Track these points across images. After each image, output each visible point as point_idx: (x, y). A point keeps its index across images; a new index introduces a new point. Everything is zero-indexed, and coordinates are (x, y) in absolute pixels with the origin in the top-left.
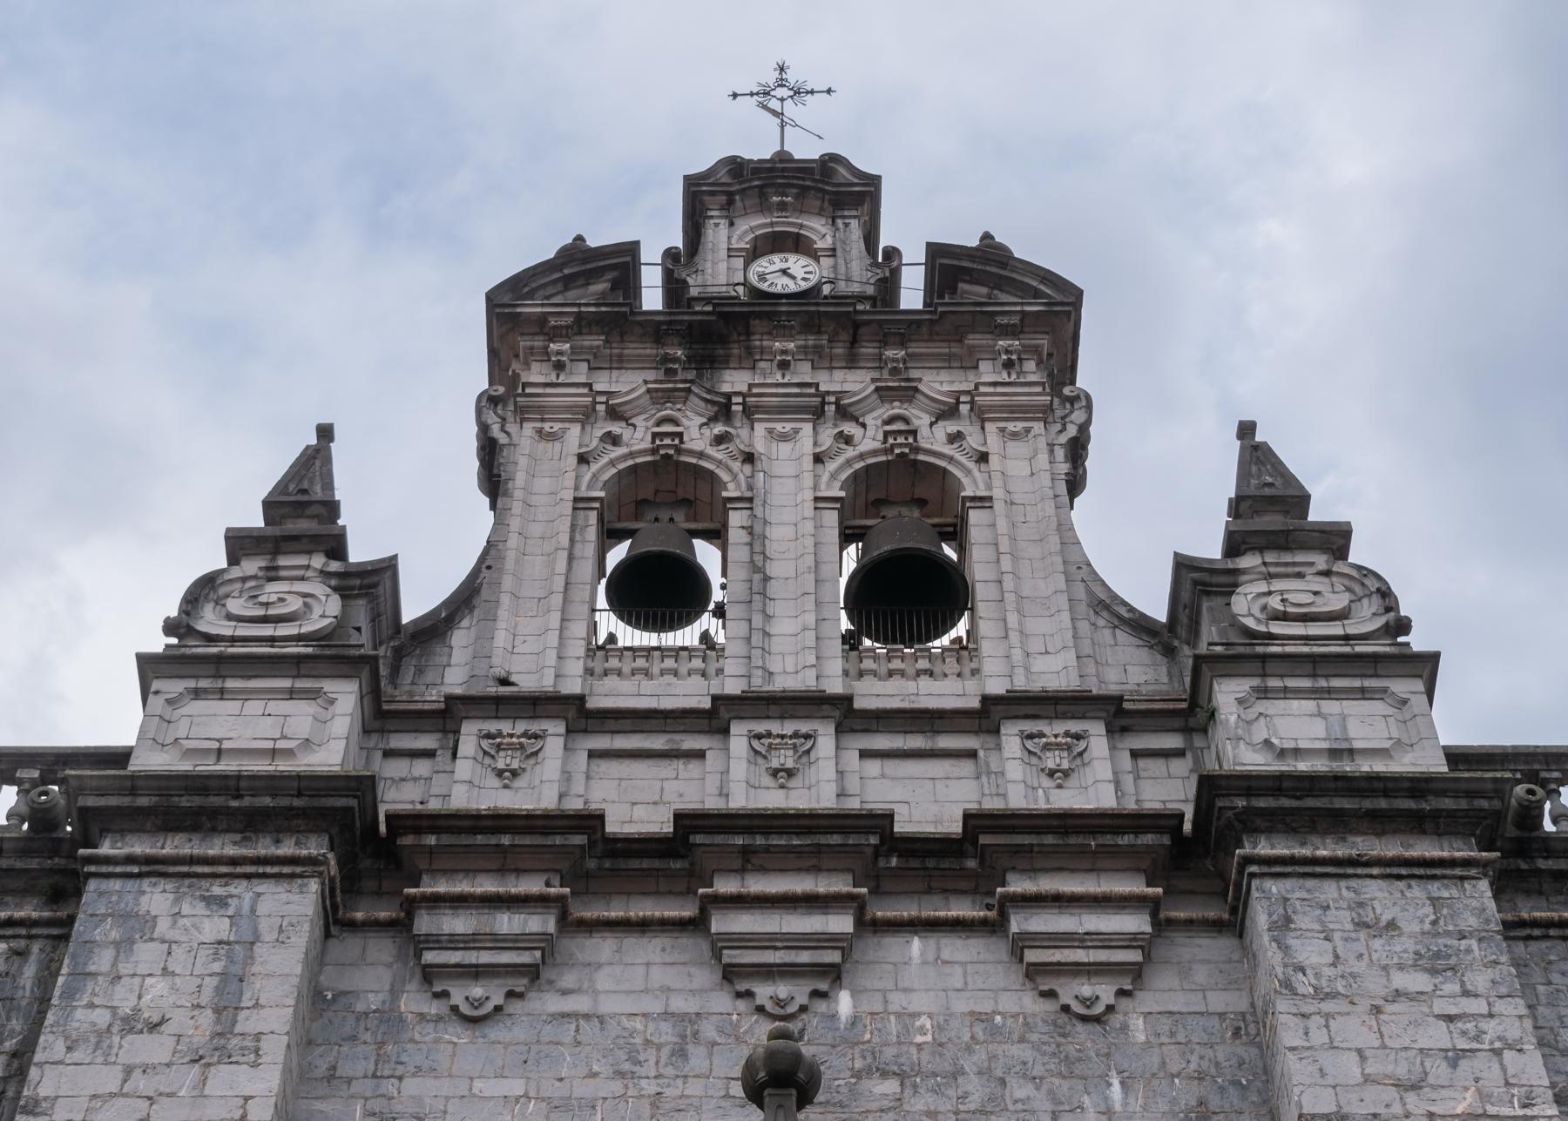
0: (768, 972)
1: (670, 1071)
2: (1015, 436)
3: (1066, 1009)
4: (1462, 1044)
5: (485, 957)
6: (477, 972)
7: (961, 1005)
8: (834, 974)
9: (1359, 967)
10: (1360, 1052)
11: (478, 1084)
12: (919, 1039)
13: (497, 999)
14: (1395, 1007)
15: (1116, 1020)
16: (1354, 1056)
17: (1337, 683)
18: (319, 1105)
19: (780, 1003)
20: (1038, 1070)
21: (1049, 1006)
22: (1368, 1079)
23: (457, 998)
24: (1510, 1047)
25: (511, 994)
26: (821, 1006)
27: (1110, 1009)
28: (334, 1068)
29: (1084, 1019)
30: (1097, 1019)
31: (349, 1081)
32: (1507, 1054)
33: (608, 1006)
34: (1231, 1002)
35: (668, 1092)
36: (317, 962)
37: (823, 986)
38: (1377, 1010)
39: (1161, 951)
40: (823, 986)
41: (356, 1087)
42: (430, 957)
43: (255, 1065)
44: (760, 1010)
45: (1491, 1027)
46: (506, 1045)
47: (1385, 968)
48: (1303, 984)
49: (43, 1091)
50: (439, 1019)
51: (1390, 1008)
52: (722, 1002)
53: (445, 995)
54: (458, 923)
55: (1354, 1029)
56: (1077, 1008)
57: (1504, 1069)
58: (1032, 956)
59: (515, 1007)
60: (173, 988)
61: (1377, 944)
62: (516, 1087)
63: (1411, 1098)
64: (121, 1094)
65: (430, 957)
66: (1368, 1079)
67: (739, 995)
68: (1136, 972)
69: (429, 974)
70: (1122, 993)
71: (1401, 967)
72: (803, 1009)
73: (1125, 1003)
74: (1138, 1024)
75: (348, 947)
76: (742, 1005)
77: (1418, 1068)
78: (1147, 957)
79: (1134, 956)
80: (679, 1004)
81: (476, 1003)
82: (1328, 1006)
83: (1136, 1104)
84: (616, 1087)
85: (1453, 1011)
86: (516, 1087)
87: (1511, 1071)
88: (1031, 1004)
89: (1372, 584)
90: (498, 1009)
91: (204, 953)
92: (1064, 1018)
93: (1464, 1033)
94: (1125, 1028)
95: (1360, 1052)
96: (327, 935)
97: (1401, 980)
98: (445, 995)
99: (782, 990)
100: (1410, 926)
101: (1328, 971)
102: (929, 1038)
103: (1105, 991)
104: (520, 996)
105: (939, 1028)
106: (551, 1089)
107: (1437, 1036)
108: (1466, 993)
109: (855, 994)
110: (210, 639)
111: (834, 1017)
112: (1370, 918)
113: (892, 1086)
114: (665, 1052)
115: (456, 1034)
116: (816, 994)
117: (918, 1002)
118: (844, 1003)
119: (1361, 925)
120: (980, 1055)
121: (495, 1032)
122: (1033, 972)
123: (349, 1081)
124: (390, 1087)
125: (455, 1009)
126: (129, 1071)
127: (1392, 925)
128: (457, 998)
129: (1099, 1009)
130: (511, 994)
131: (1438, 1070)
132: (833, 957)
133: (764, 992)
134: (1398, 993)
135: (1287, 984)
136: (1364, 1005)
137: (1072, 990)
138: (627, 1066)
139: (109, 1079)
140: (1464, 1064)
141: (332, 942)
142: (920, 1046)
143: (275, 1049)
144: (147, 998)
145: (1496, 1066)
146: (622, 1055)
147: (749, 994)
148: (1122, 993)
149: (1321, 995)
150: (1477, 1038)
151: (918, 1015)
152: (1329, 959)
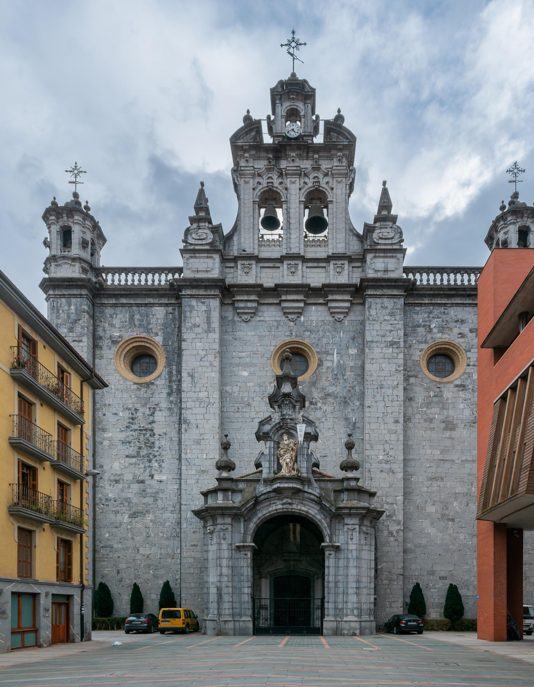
2: (339, 182)
17: (388, 255)
20: (331, 330)
30: (340, 321)
34: (360, 318)
49: (185, 337)
54: (242, 305)
61: (384, 311)
83: (344, 336)
89: (399, 231)
91: (203, 313)
100: (389, 307)
101: (375, 316)
110: (191, 244)
112: (383, 306)
124: (235, 333)
126: (196, 334)
128: (243, 318)
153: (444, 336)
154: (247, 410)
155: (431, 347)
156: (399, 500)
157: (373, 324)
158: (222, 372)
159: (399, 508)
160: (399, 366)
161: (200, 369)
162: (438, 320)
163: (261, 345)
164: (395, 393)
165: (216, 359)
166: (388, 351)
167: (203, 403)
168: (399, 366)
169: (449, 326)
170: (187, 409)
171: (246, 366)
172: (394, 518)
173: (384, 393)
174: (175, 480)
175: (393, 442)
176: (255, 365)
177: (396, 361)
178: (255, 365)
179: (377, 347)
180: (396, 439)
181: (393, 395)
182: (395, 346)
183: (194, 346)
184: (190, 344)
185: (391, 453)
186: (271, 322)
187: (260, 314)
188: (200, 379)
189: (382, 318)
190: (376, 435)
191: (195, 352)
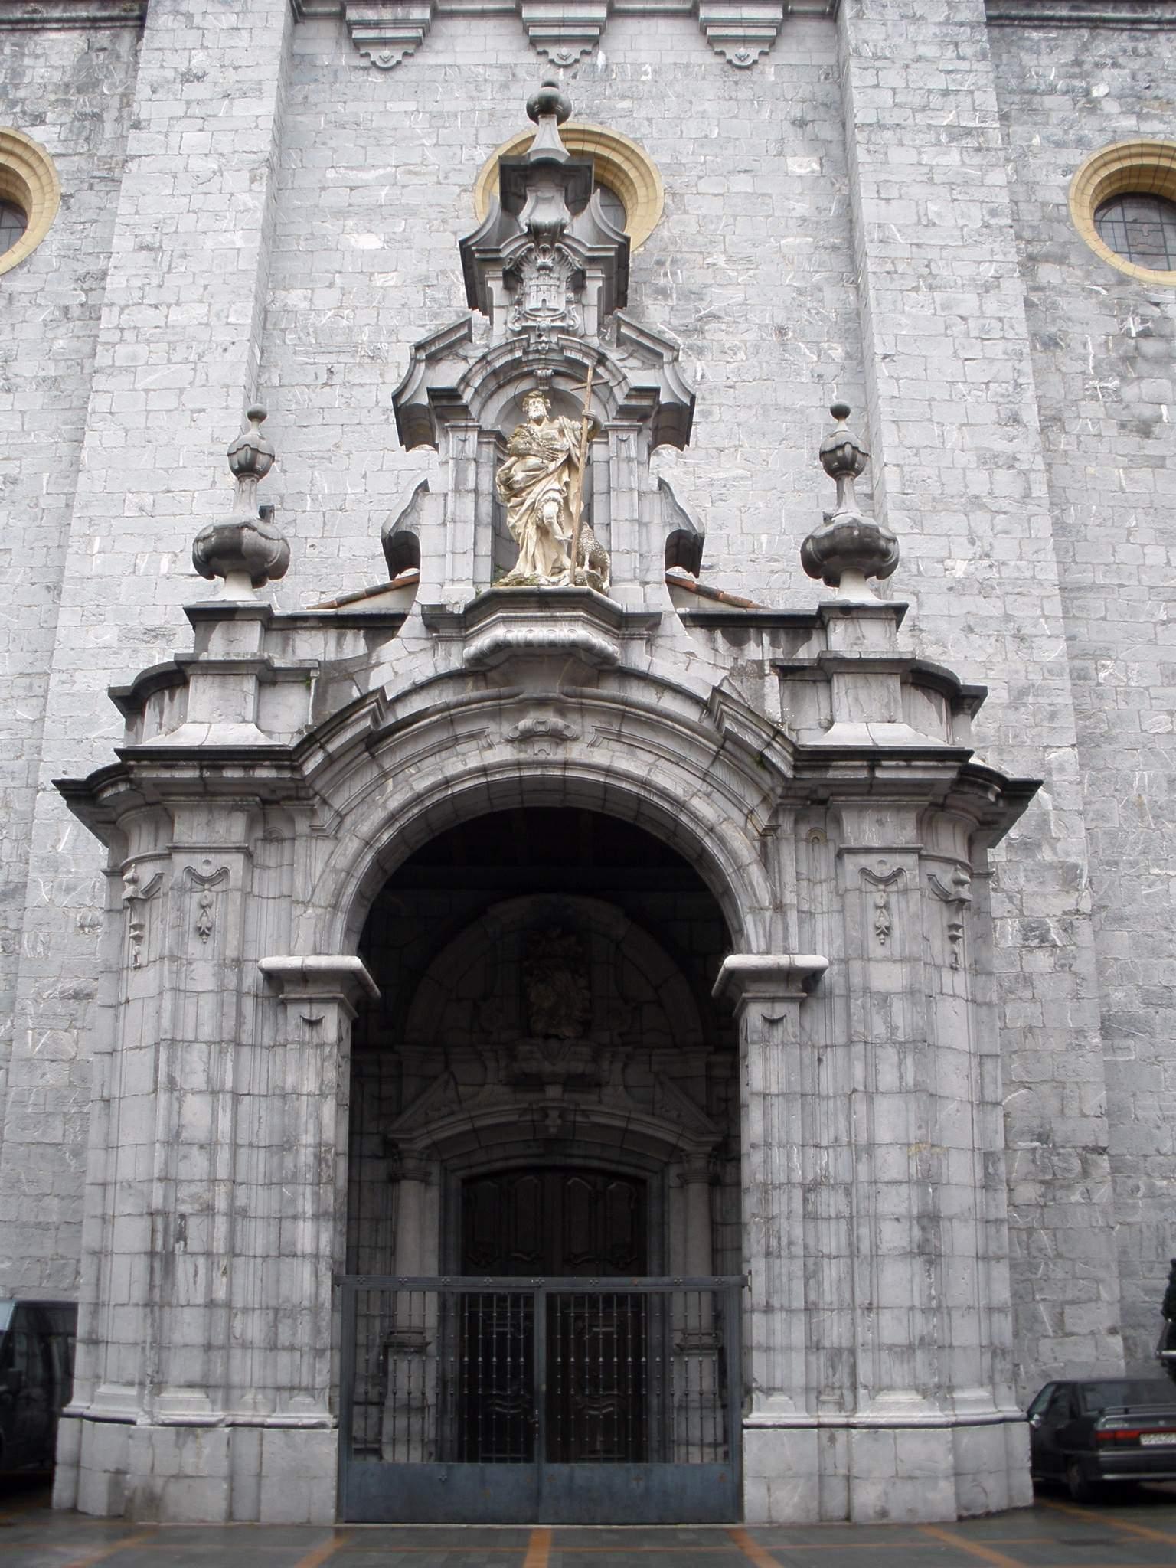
0: (559, 40)
1: (498, 96)
3: (730, 62)
4: (952, 87)
5: (389, 34)
6: (385, 42)
7: (669, 59)
8: (595, 41)
9: (900, 41)
10: (894, 90)
11: (389, 105)
12: (644, 78)
13: (398, 57)
14: (918, 65)
15: (757, 69)
16: (890, 93)
18: (299, 118)
19: (562, 58)
21: (720, 60)
22: (896, 105)
23: (374, 57)
24: (978, 89)
25: (405, 54)
26: (587, 60)
27: (755, 62)
28: (306, 97)
29: (740, 68)
31: (316, 105)
32: (977, 93)
33: (460, 62)
35: (498, 107)
36: (290, 37)
37: (588, 48)
38: (907, 66)
39: (788, 29)
40: (588, 48)
41: (319, 108)
42: (358, 34)
43: (260, 98)
44: (552, 61)
45: (970, 79)
46: (404, 83)
47: (915, 43)
48: (867, 51)
50: (364, 69)
51: (913, 65)
52: (530, 57)
53: (367, 55)
55: (893, 77)
56: (736, 62)
57: (974, 102)
58: (711, 32)
59: (408, 61)
60: (209, 56)
61: (912, 29)
62: (411, 106)
63: (919, 116)
64: (186, 116)
65: (358, 34)
66: (896, 105)
67: (539, 53)
68: (772, 42)
69: (357, 44)
70: (762, 53)
71: (924, 42)
72: (577, 61)
73: (763, 59)
74: (770, 71)
75: (311, 28)
76: (542, 59)
77: (925, 99)
78: (779, 32)
79: (772, 32)
80: (504, 59)
81: (385, 60)
82: (878, 64)
84: (469, 105)
85: (951, 68)
86: (411, 106)
87: (977, 103)
88: (709, 58)
90: (399, 63)
92: (728, 67)
93: (954, 80)
94: (762, 73)
95: (894, 90)
96: (296, 22)
97: (922, 50)
98: (367, 55)
99: (564, 50)
102: (649, 77)
103: (753, 53)
104: (412, 55)
105: (655, 71)
106: (431, 106)
107: (939, 82)
108: (959, 58)
109: (605, 52)
111: (594, 65)
112: (910, 13)
113: (626, 104)
114: (497, 86)
115: (376, 78)
116: (584, 53)
117: (644, 57)
118: (601, 58)
119: (903, 17)
120: (678, 88)
121: (398, 74)
122: (712, 41)
123: (316, 105)
125: (374, 63)
126: (188, 103)
127: (922, 18)
128: (374, 57)
129: (748, 62)
130: (405, 54)
131: (936, 101)
132: (596, 32)
133: (554, 52)
134: (919, 59)
135: (856, 50)
136: (899, 64)
137: (732, 52)
138: (475, 94)
139: (179, 109)
140: (952, 97)
141: (300, 26)
142: (644, 82)
143: (271, 89)
144: (194, 62)
145: (969, 100)
146: (472, 87)
147: (545, 53)
148: (762, 53)
149: (876, 57)
150: (961, 84)
151: (644, 64)
152: (883, 36)
153: (1147, 127)
154: (366, 380)
155: (1104, 161)
156: (1061, 769)
157: (878, 70)
158: (273, 235)
159: (1065, 804)
160: (993, 213)
161: (187, 223)
162: (1115, 71)
163: (437, 145)
164: (991, 306)
165: (255, 186)
166: (944, 160)
167: (181, 348)
168: (993, 213)
169: (1160, 93)
170: (112, 370)
171: (374, 214)
172: (1046, 855)
173: (944, 307)
174: (26, 681)
175: (1004, 505)
176: (412, 212)
177: (979, 194)
178: (412, 212)
179: (901, 144)
180: (1017, 491)
181: (982, 315)
182: (970, 142)
183: (174, 139)
184: (161, 137)
185: (1004, 549)
186: (481, 70)
187: (439, 44)
188: (184, 256)
189: (908, 53)
190: (933, 472)
191: (177, 164)
